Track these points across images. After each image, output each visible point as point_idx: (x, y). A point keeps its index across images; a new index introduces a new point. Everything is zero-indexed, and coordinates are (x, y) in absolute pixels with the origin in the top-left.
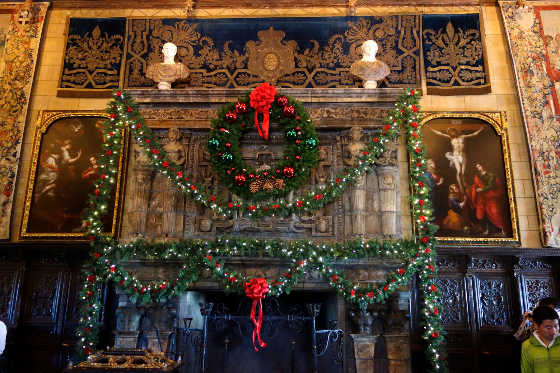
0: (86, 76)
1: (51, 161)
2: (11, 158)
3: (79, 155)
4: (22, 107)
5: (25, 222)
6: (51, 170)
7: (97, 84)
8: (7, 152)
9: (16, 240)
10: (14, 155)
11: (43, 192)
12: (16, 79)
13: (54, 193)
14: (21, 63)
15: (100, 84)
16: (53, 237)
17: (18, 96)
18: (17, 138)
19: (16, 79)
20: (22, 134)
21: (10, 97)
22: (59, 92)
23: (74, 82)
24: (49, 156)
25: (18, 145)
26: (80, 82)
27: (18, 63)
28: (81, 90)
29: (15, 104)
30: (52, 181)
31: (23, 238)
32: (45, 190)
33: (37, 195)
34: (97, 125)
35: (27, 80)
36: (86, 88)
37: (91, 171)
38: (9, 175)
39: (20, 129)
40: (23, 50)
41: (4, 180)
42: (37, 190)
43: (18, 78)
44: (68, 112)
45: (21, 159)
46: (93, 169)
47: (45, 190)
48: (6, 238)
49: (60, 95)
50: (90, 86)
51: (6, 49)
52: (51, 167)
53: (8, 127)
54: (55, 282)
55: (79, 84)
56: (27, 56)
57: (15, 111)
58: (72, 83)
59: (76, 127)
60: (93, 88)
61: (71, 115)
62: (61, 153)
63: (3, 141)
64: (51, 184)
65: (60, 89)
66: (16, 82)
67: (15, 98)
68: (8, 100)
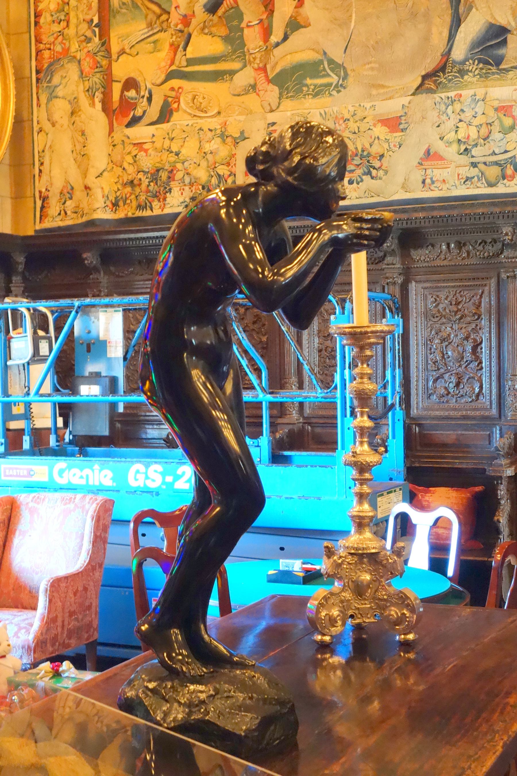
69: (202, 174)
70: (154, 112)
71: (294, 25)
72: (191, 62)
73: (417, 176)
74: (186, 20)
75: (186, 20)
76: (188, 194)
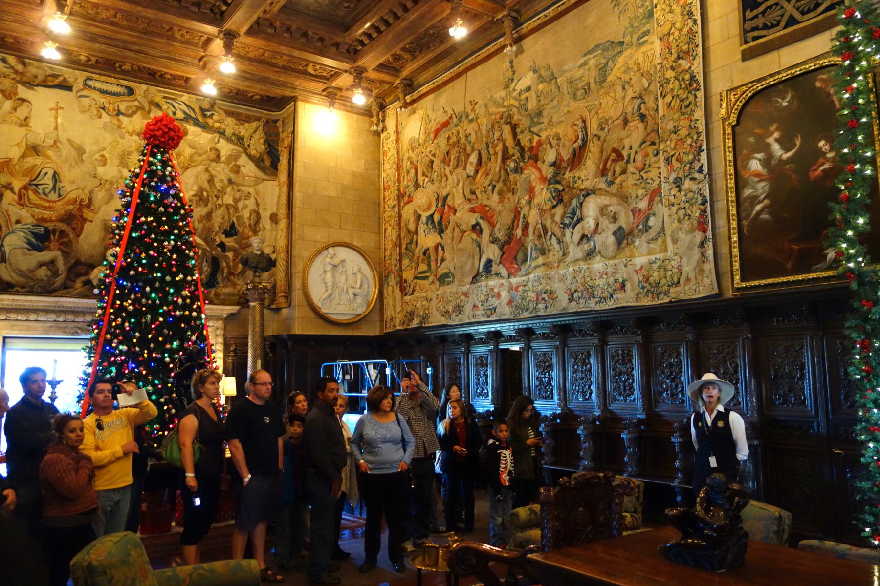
0: (782, 7)
1: (755, 165)
2: (697, 175)
3: (798, 142)
4: (696, 97)
5: (737, 266)
6: (757, 179)
7: (803, 13)
8: (690, 168)
9: (729, 294)
10: (700, 171)
11: (752, 216)
12: (679, 58)
13: (770, 213)
14: (680, 30)
15: (809, 11)
16: (783, 283)
17: (687, 82)
18: (698, 145)
19: (679, 58)
20: (703, 136)
21: (677, 88)
22: (743, 52)
23: (765, 27)
24: (749, 158)
25: (702, 154)
26: (775, 22)
27: (677, 33)
28: (779, 34)
29: (685, 96)
30: (763, 197)
31: (739, 289)
32: (754, 212)
33: (745, 223)
34: (818, 84)
35: (694, 54)
36: (785, 27)
37: (823, 164)
38: (699, 202)
39: (700, 130)
40: (678, 10)
41: (694, 210)
42: (743, 215)
43: (681, 55)
44: (764, 79)
45: (710, 174)
46: (827, 160)
47: (754, 212)
48: (714, 293)
49: (747, 56)
50: (792, 21)
51: (657, 20)
52: (757, 175)
53: (683, 132)
54: (799, 353)
55: (773, 26)
56: (687, 17)
57: (688, 106)
58: (761, 29)
59: (783, 99)
60: (798, 22)
61: (771, 81)
62: (766, 148)
63: (682, 155)
64: (762, 202)
65: (745, 47)
66: (680, 61)
67: (683, 86)
68: (675, 93)
69: (421, 313)
70: (410, 292)
71: (443, 260)
72: (419, 273)
73: (471, 314)
74: (418, 258)
75: (418, 258)
76: (419, 320)
